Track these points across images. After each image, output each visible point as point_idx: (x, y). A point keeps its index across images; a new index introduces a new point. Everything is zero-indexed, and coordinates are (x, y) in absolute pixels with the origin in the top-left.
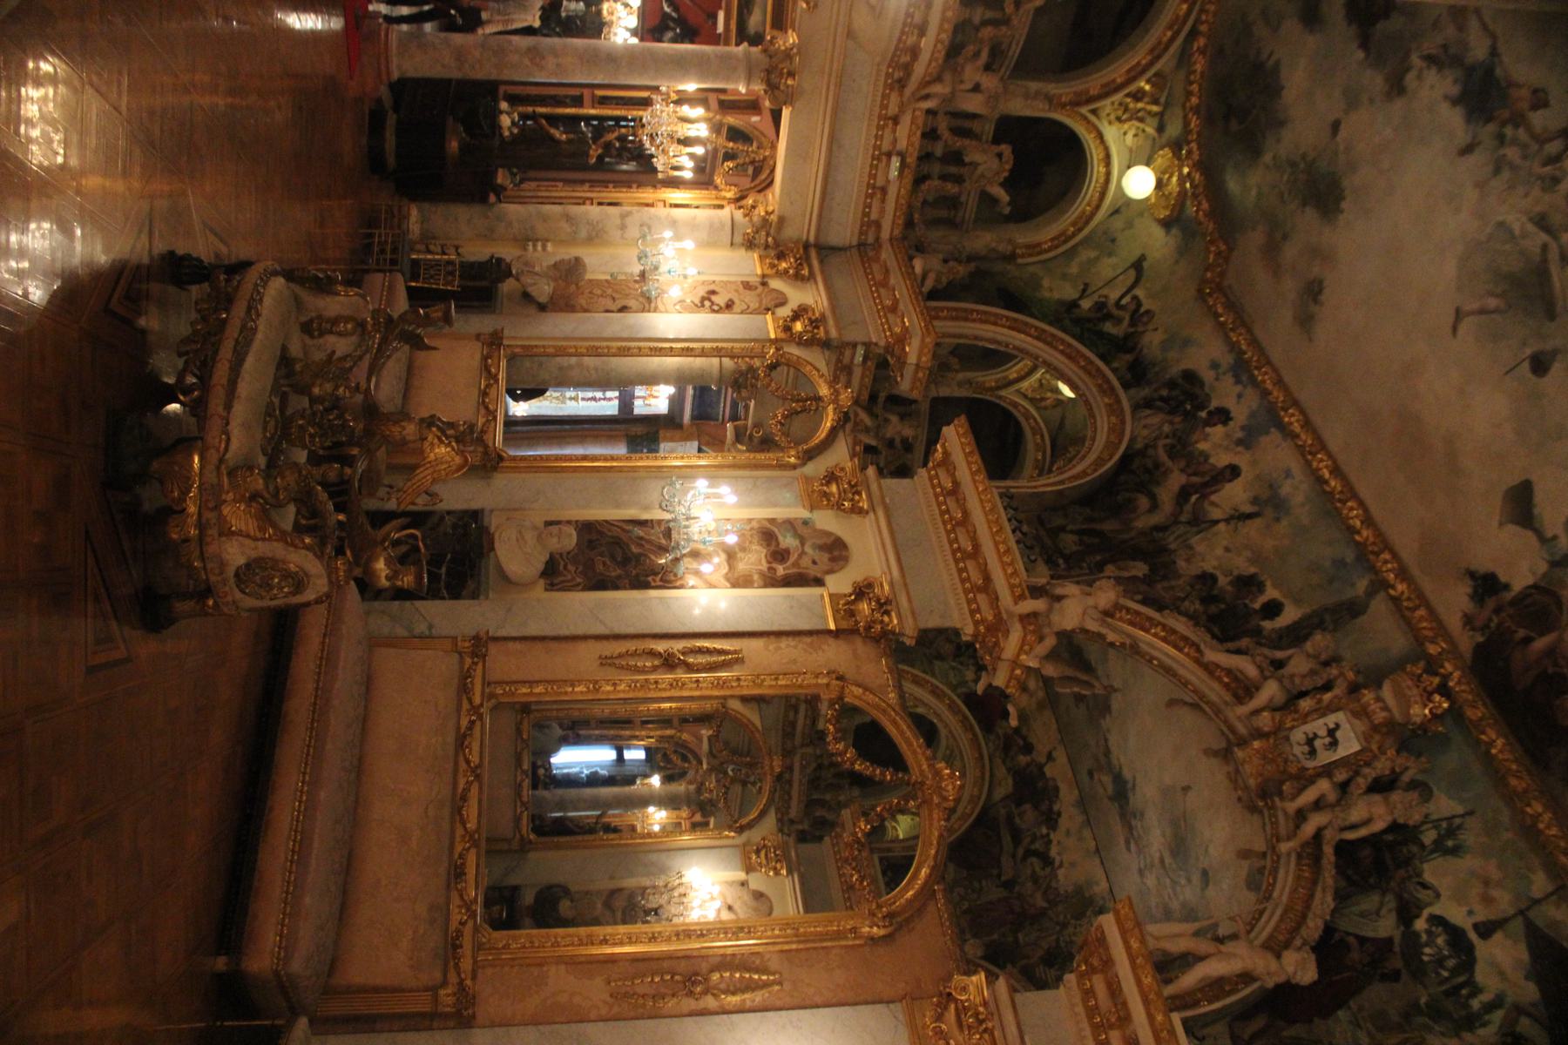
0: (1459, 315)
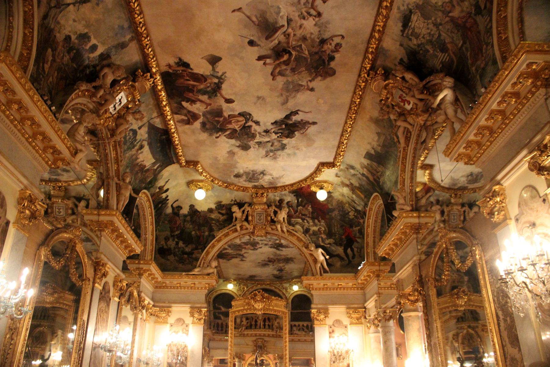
0: (240, 9)
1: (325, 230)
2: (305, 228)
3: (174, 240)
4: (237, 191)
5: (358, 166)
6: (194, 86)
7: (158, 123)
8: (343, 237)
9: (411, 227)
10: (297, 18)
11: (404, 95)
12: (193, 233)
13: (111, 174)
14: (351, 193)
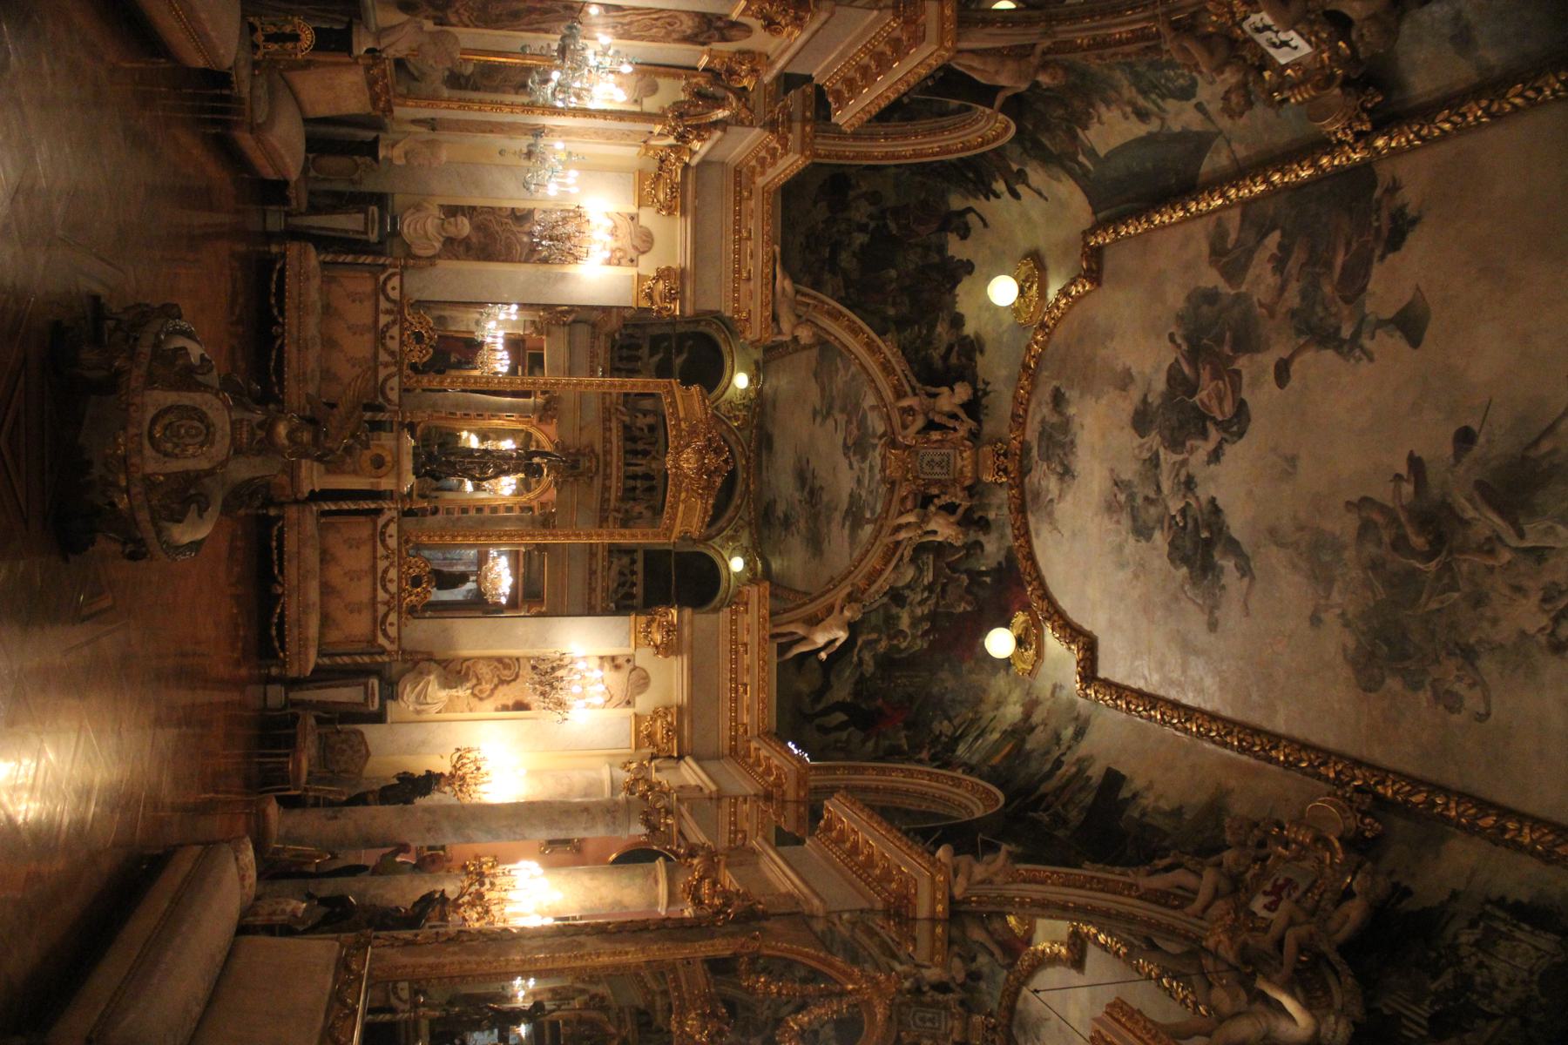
1: (900, 651)
2: (907, 592)
3: (871, 217)
4: (1014, 397)
5: (1083, 748)
6: (1329, 265)
7: (1216, 161)
8: (880, 702)
9: (905, 897)
10: (1546, 578)
11: (1296, 895)
12: (893, 273)
13: (1060, 28)
14: (1005, 726)
